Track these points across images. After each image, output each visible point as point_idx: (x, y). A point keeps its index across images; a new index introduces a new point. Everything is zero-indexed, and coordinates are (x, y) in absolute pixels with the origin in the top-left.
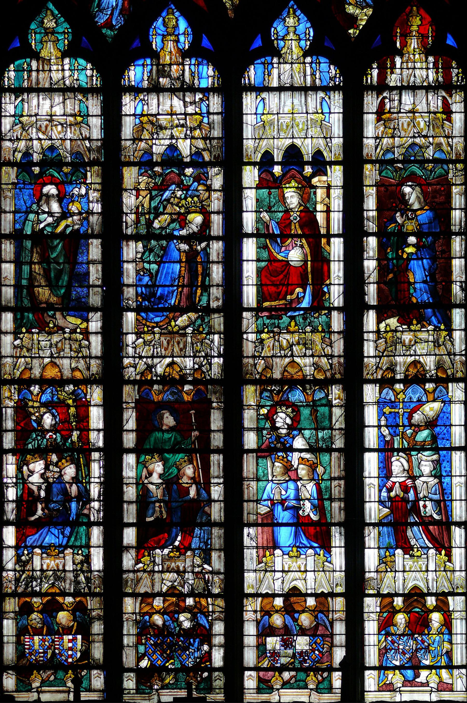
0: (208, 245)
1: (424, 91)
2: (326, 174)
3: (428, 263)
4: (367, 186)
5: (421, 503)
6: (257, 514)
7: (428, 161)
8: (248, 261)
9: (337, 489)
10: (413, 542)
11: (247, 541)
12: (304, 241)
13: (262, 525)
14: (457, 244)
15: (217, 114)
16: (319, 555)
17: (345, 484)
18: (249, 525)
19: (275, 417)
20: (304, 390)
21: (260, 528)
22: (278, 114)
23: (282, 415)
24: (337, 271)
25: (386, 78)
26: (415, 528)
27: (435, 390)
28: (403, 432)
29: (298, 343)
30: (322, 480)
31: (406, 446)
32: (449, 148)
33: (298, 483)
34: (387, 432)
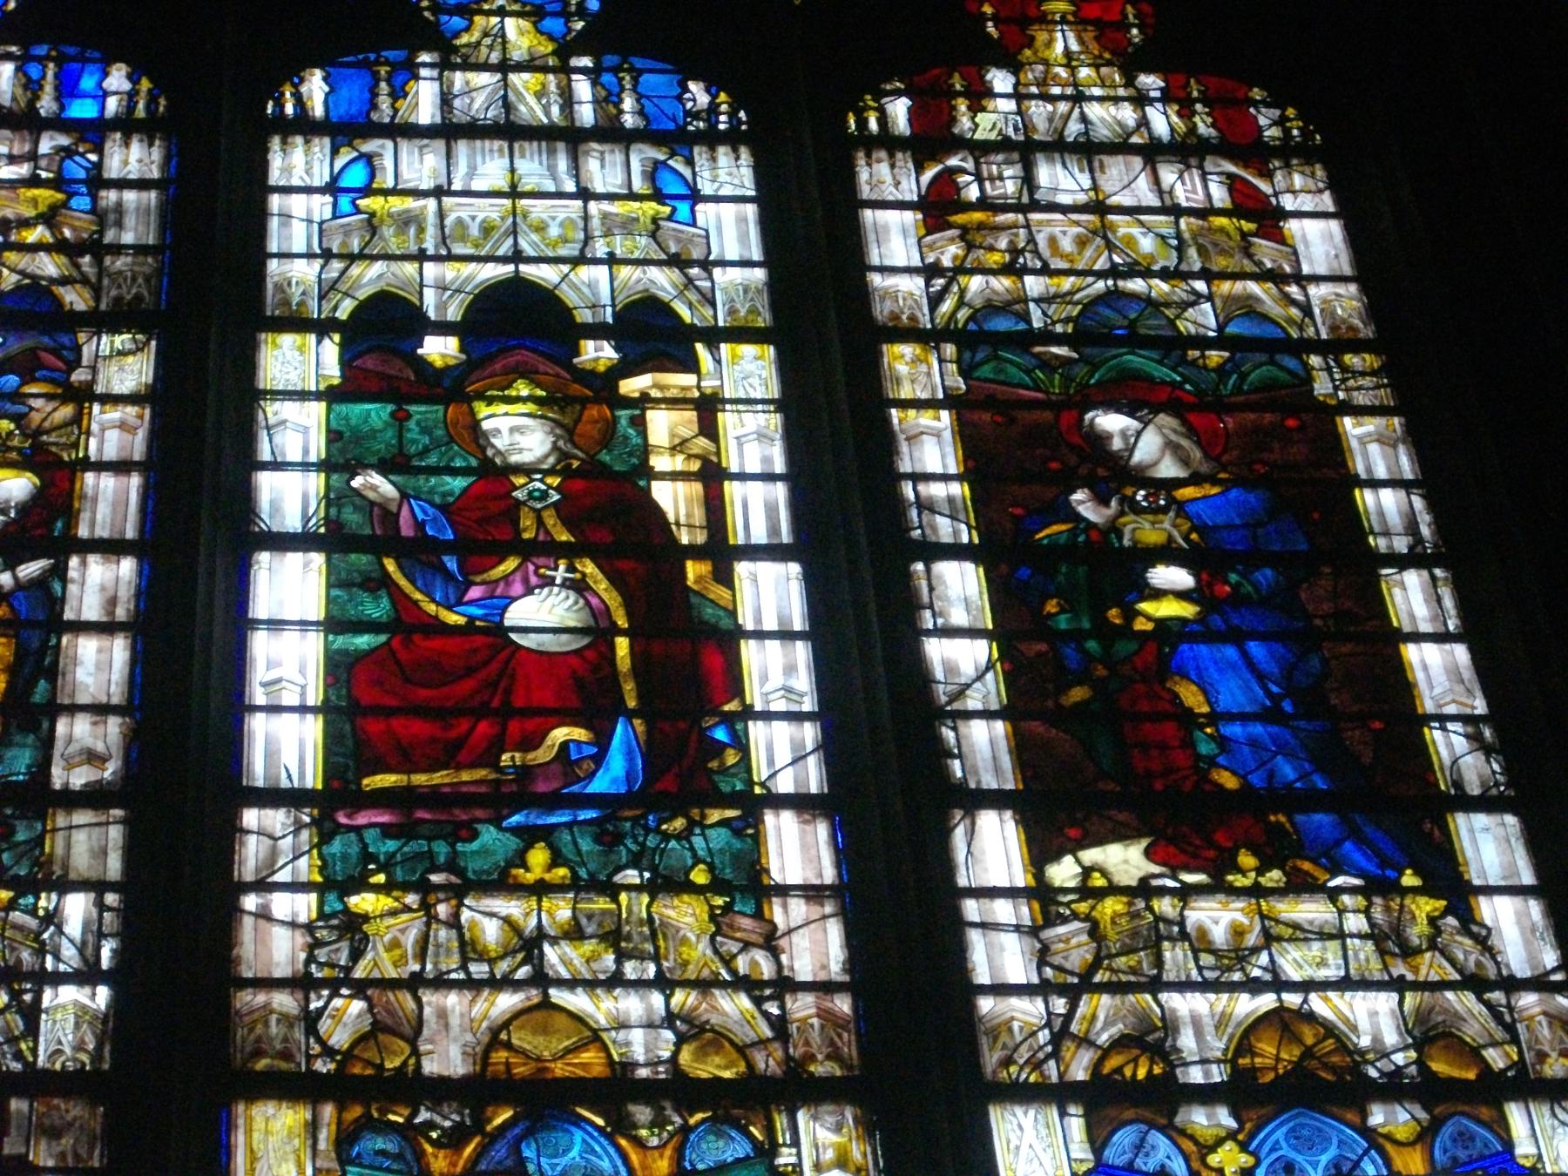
0: (60, 572)
1: (1137, 162)
2: (692, 366)
3: (1271, 653)
4: (905, 404)
7: (1202, 343)
8: (276, 625)
12: (589, 567)
14: (1411, 597)
15: (141, 184)
20: (620, 1126)
22: (439, 192)
24: (777, 672)
25: (953, 120)
29: (574, 933)
32: (1294, 312)
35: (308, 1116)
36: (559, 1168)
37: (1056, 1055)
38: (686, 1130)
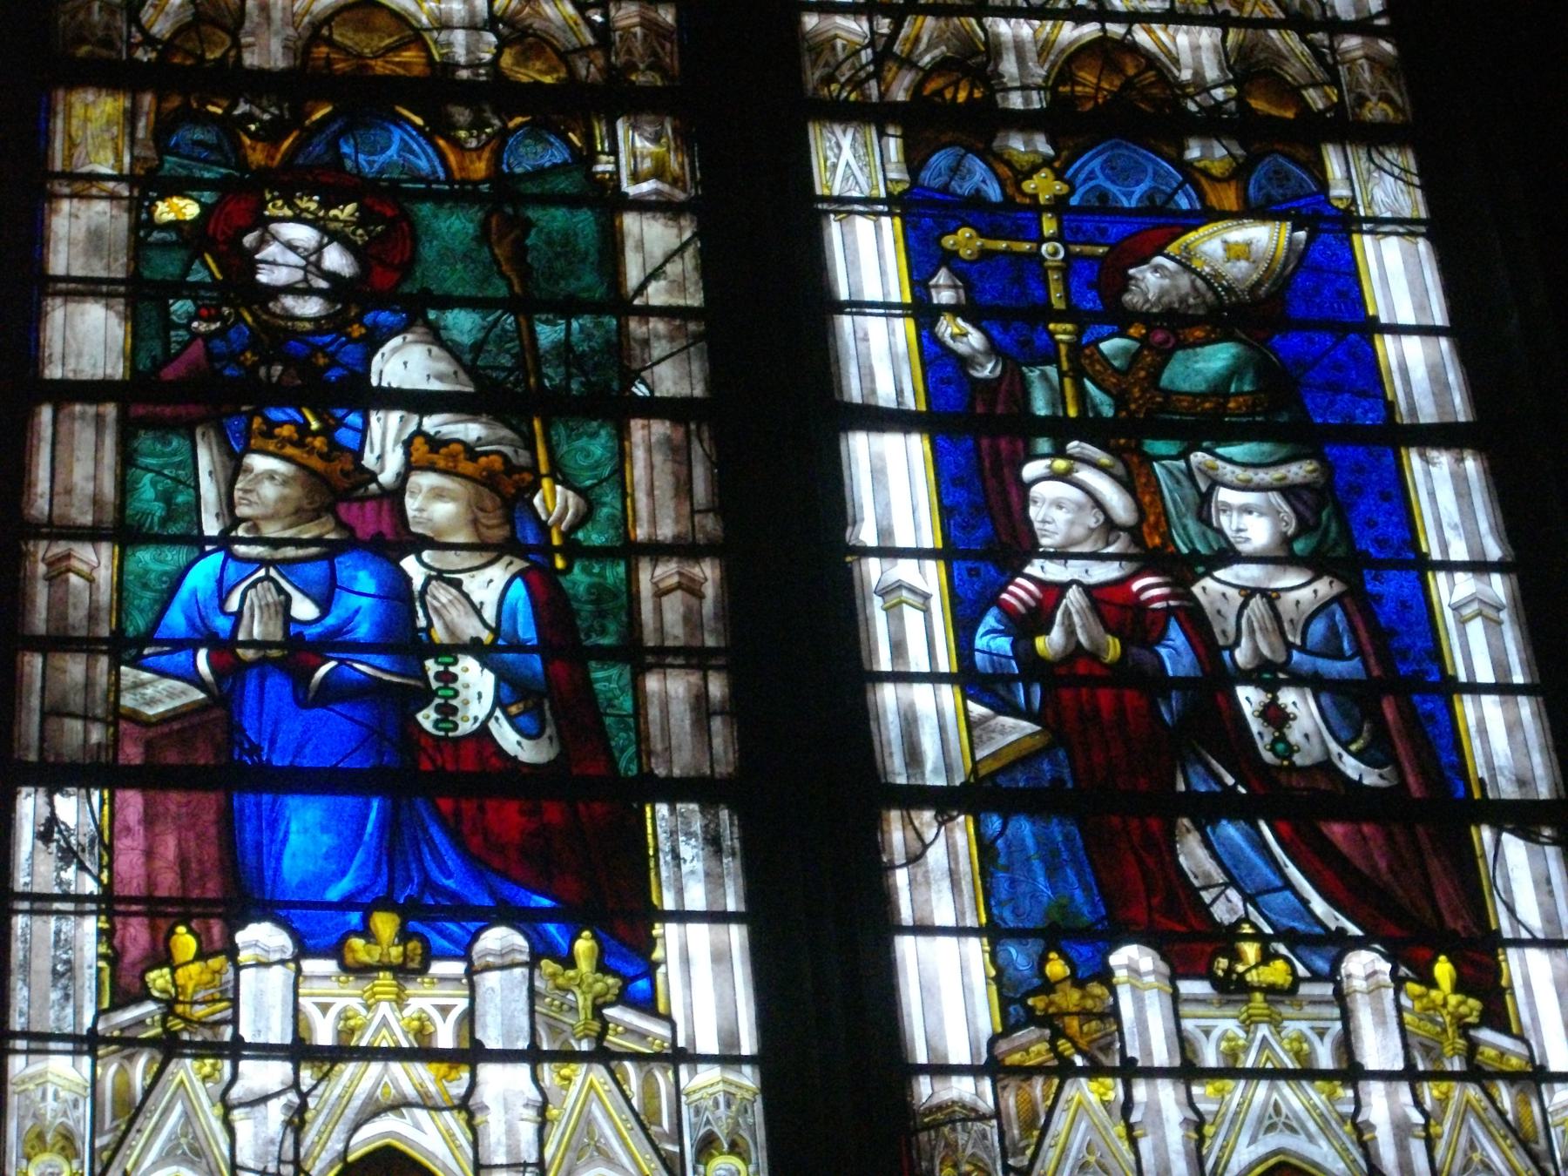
5: (1249, 698)
6: (116, 716)
9: (673, 596)
10: (1227, 907)
11: (33, 866)
13: (150, 778)
16: (569, 961)
17: (728, 581)
18: (57, 775)
19: (249, 240)
20: (439, 127)
21: (133, 802)
23: (303, 235)
26: (1230, 831)
27: (1239, 173)
28: (1075, 348)
30: (573, 550)
31: (1107, 411)
33: (409, 564)
34: (975, 339)
35: (128, 104)
36: (376, 166)
37: (878, 75)
38: (504, 134)
